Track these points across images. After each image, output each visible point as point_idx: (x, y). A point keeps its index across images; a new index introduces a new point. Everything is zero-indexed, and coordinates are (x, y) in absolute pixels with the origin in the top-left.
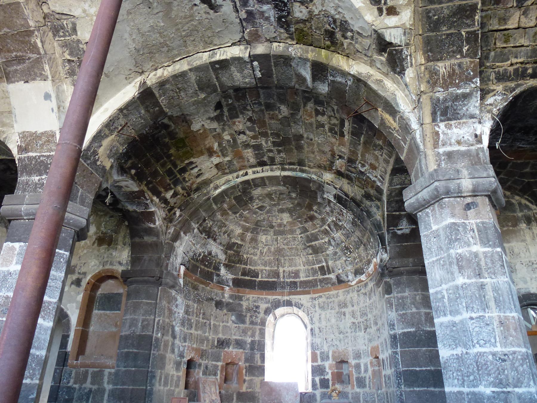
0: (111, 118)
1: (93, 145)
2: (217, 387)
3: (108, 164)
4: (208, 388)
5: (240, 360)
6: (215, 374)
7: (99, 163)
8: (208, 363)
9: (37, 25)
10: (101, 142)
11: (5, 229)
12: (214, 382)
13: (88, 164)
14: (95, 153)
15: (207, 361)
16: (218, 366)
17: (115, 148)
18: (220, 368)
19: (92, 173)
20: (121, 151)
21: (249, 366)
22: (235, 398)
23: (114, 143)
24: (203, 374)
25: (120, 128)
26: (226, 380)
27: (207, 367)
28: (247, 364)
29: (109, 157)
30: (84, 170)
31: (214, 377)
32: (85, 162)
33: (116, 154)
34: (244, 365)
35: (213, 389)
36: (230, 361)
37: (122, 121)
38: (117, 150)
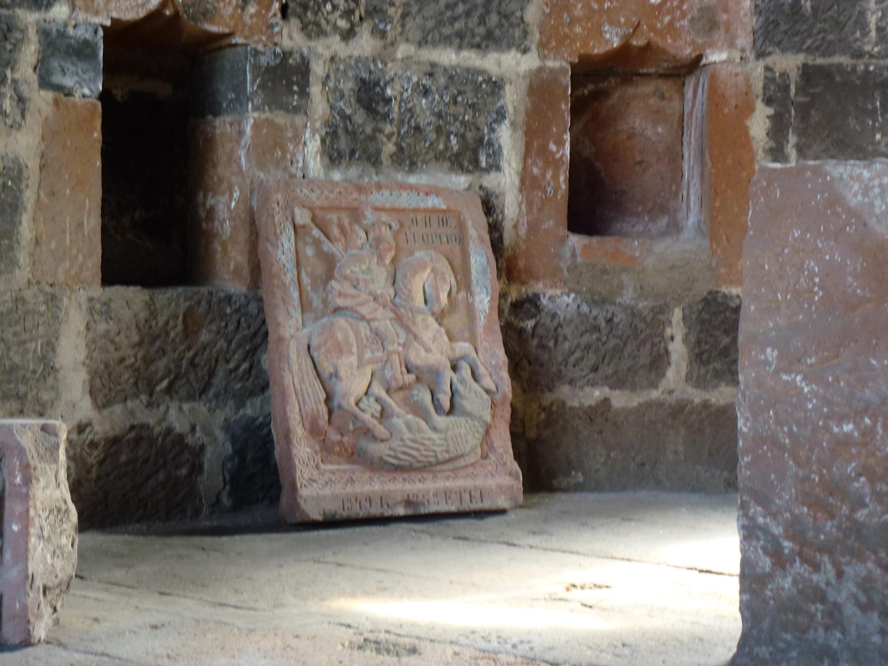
2: (480, 259)
4: (365, 272)
5: (709, 23)
6: (472, 155)
8: (382, 57)
12: (443, 216)
15: (365, 44)
16: (496, 86)
18: (512, 98)
21: (808, 73)
22: (678, 350)
24: (333, 156)
26: (593, 202)
27: (370, 94)
28: (789, 63)
31: (461, 181)
34: (757, 70)
35: (427, 278)
36: (613, 38)
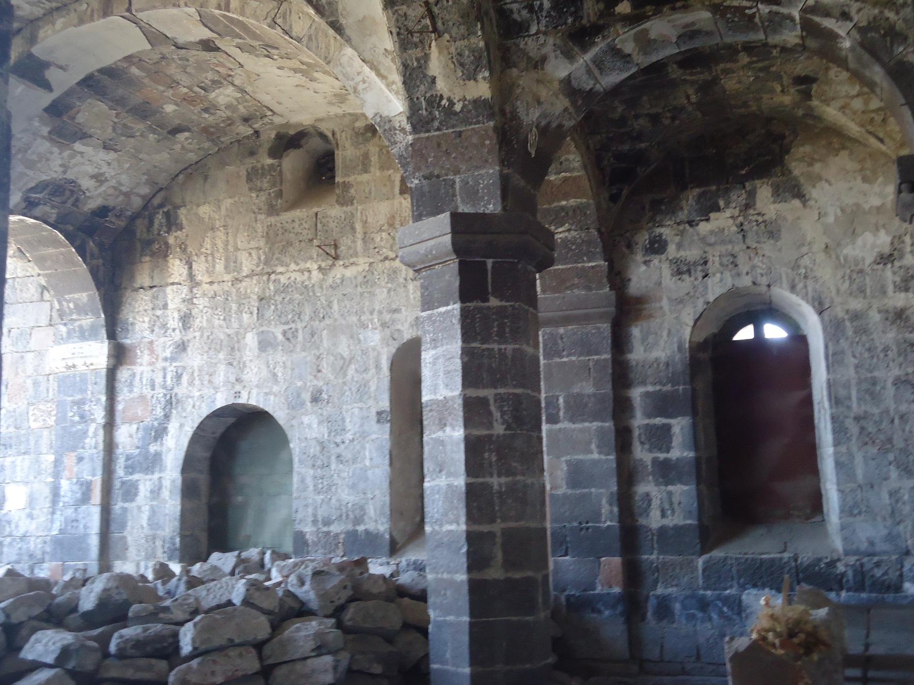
0: (394, 31)
1: (418, 95)
3: (482, 89)
7: (458, 107)
9: (269, 20)
10: (425, 76)
11: (796, 203)
13: (438, 129)
14: (434, 101)
17: (467, 53)
19: (460, 134)
20: (482, 44)
23: (453, 50)
25: (428, 21)
29: (471, 76)
30: (439, 145)
32: (428, 131)
33: (478, 59)
37: (416, 11)
38: (473, 51)
